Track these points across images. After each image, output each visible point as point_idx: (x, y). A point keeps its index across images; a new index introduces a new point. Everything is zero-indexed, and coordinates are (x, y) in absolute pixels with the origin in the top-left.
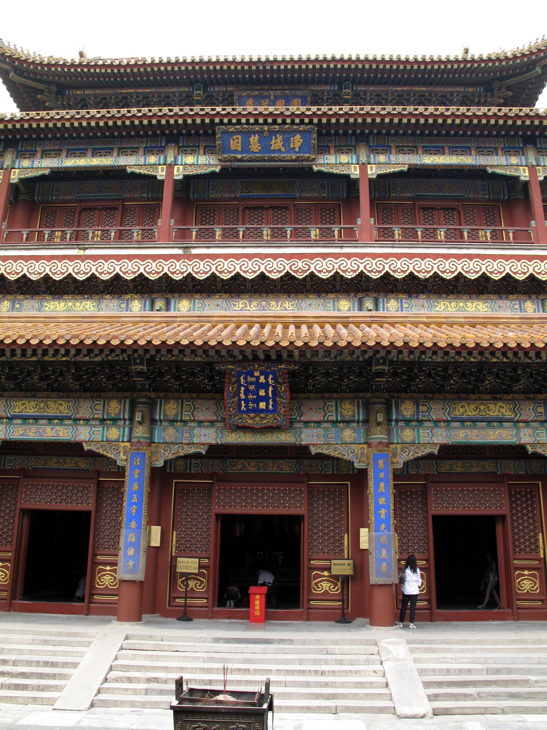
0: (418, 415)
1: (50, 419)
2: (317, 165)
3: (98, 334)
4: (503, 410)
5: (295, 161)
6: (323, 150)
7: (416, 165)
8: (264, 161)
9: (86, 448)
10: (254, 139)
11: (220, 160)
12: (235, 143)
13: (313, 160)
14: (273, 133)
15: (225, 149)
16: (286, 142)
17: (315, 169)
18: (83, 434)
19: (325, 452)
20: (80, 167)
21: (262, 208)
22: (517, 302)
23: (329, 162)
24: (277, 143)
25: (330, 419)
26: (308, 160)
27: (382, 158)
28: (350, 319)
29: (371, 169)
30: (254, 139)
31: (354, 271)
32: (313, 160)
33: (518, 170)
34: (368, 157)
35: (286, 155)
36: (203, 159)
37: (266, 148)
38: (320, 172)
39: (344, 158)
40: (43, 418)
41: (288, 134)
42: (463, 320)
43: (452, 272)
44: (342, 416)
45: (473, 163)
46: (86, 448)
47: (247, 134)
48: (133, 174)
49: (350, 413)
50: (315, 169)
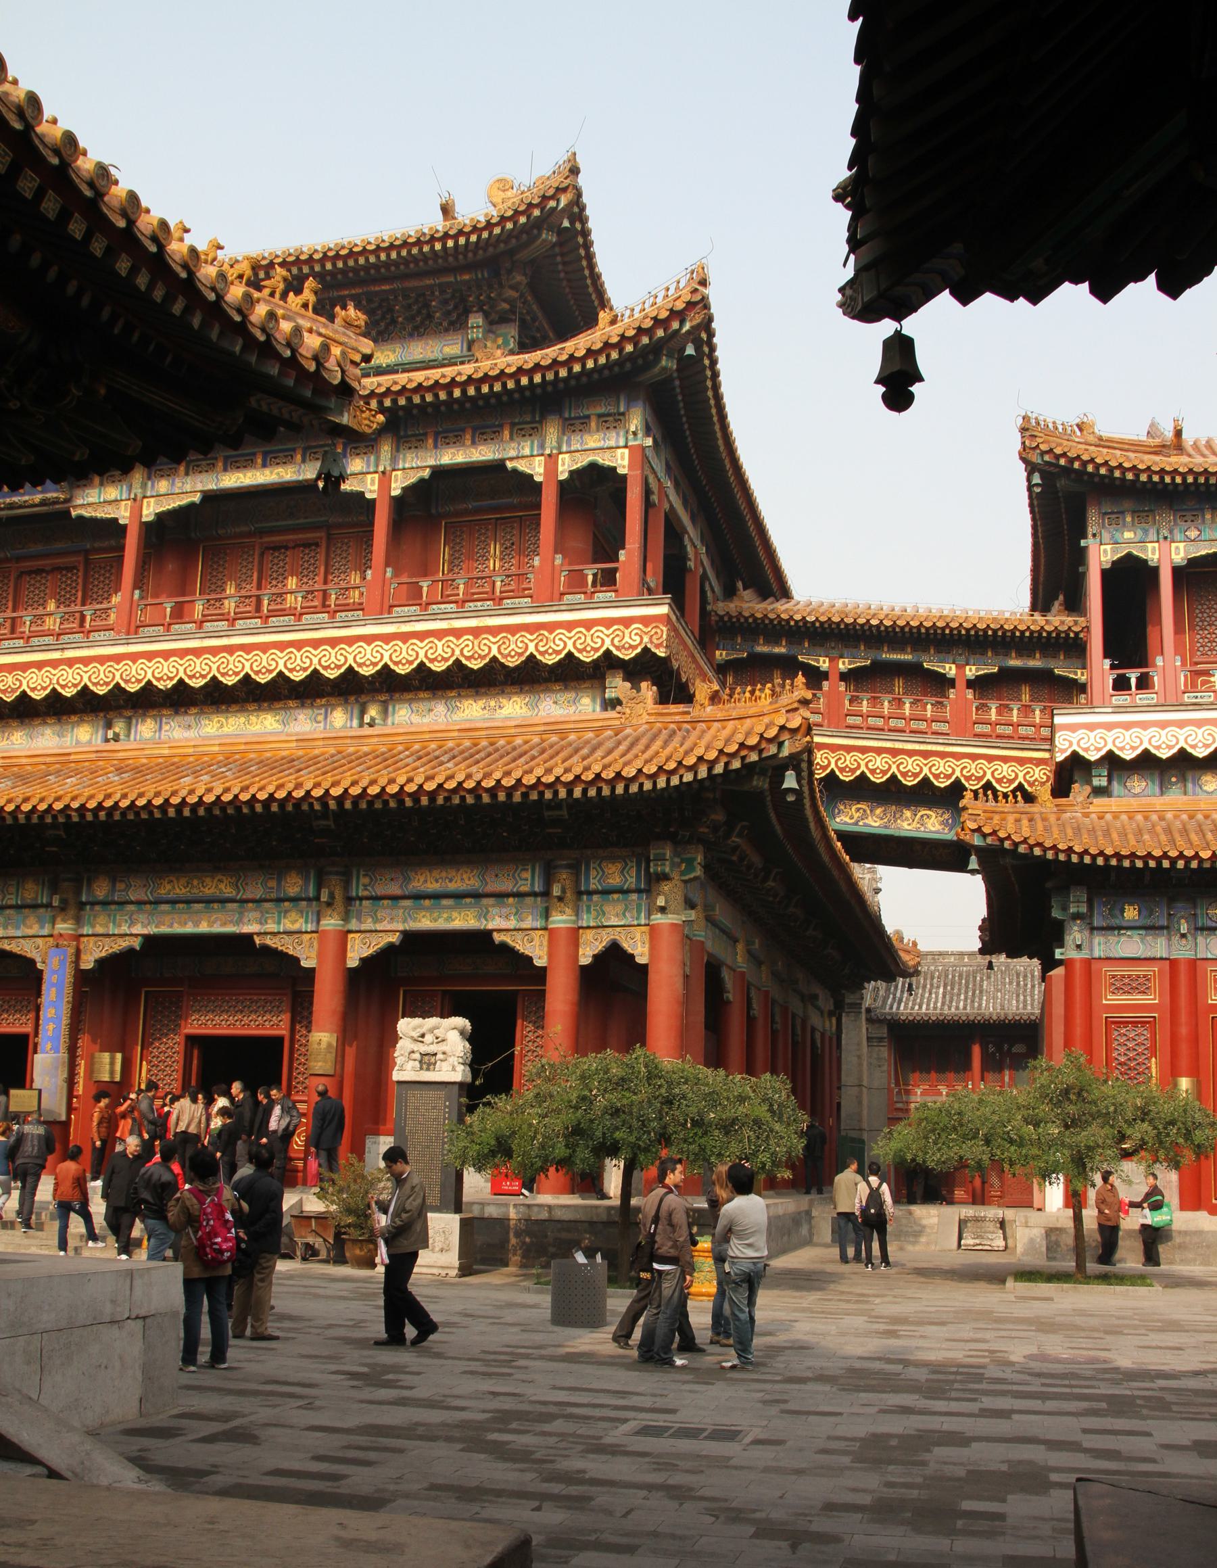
0: (113, 895)
2: (75, 507)
4: (222, 886)
7: (212, 491)
13: (67, 501)
21: (39, 571)
22: (323, 711)
23: (91, 500)
25: (9, 903)
26: (56, 501)
27: (163, 486)
28: (72, 757)
29: (149, 505)
31: (75, 686)
32: (67, 501)
33: (363, 481)
34: (144, 486)
35: (26, 498)
38: (81, 518)
39: (112, 492)
42: (216, 749)
43: (204, 677)
44: (23, 899)
45: (295, 478)
49: (32, 895)
50: (74, 513)
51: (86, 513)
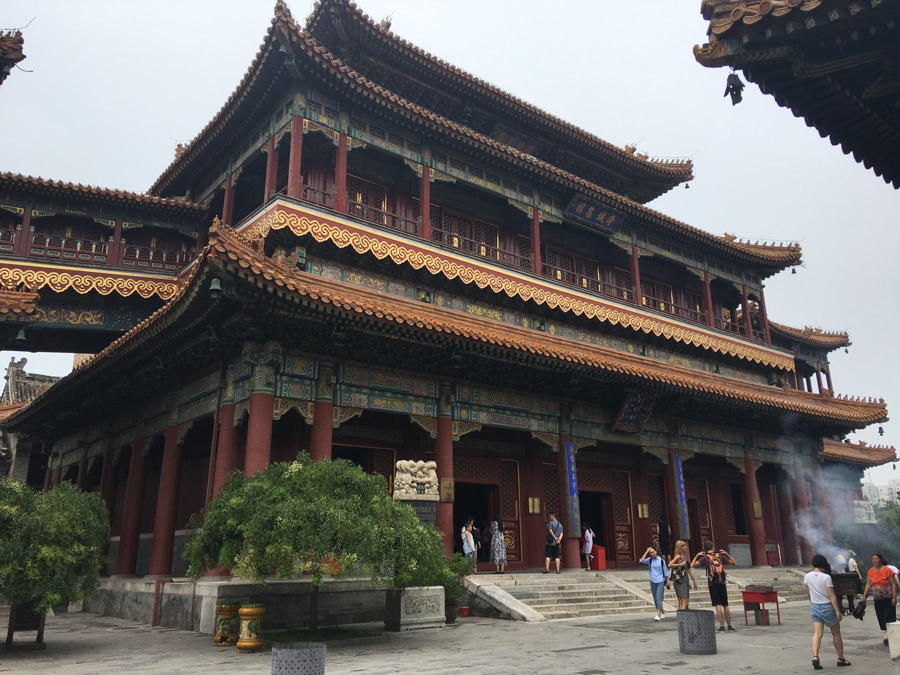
1: (512, 410)
3: (600, 361)
5: (606, 232)
6: (616, 228)
8: (589, 226)
9: (534, 436)
10: (591, 209)
11: (564, 216)
12: (580, 209)
13: (611, 233)
14: (603, 210)
15: (573, 210)
16: (607, 218)
17: (611, 240)
18: (534, 425)
19: (650, 451)
20: (479, 186)
24: (601, 217)
30: (591, 209)
36: (554, 211)
37: (594, 218)
38: (612, 243)
39: (626, 238)
40: (509, 409)
41: (610, 212)
46: (534, 436)
47: (589, 204)
48: (512, 205)
51: (615, 243)
